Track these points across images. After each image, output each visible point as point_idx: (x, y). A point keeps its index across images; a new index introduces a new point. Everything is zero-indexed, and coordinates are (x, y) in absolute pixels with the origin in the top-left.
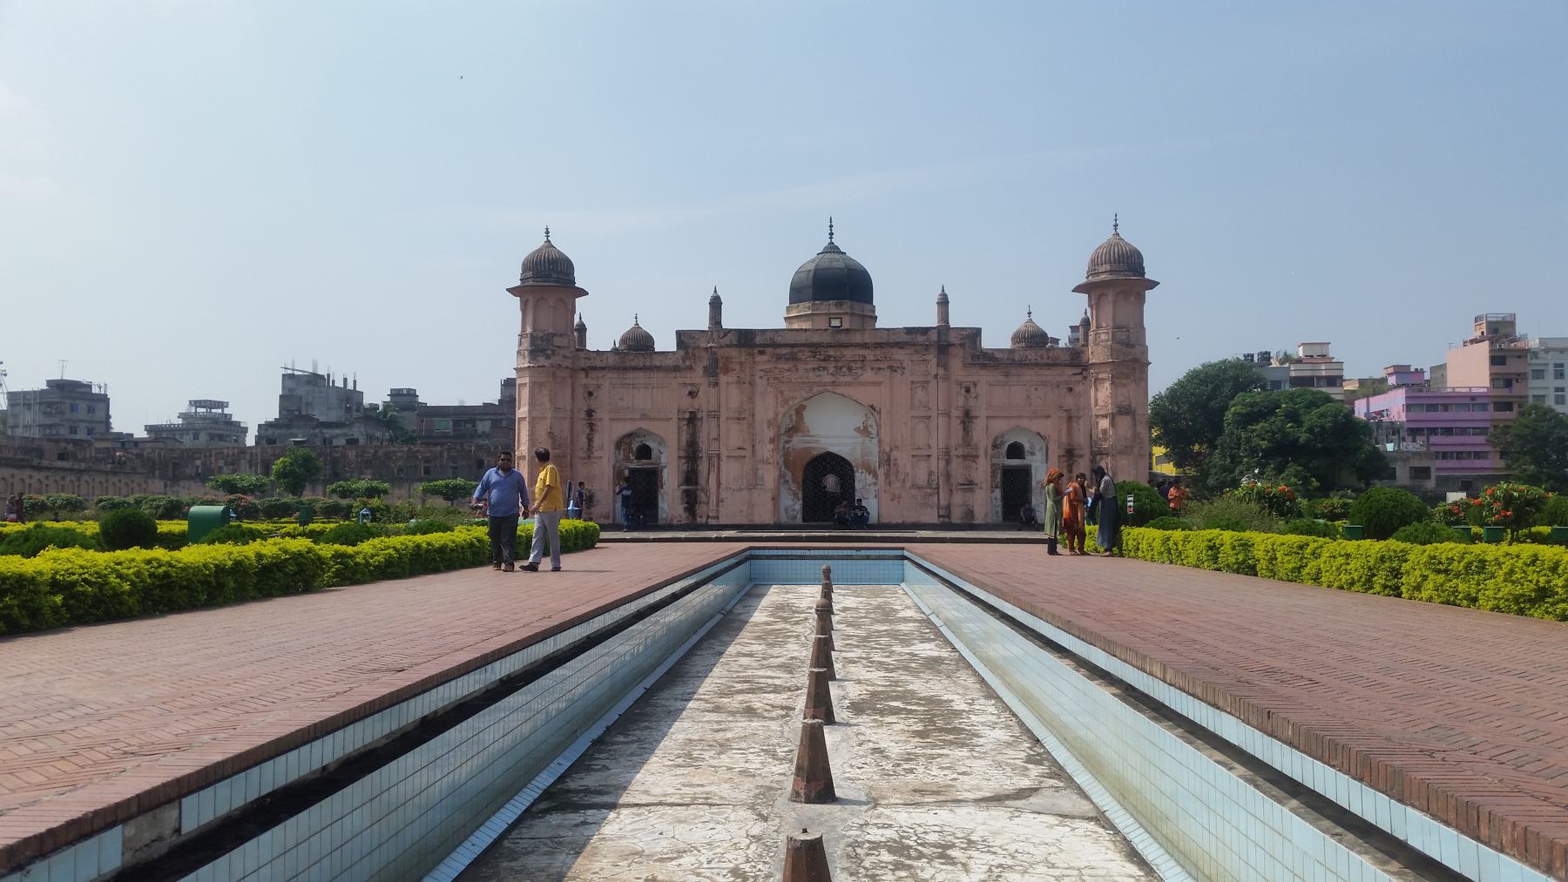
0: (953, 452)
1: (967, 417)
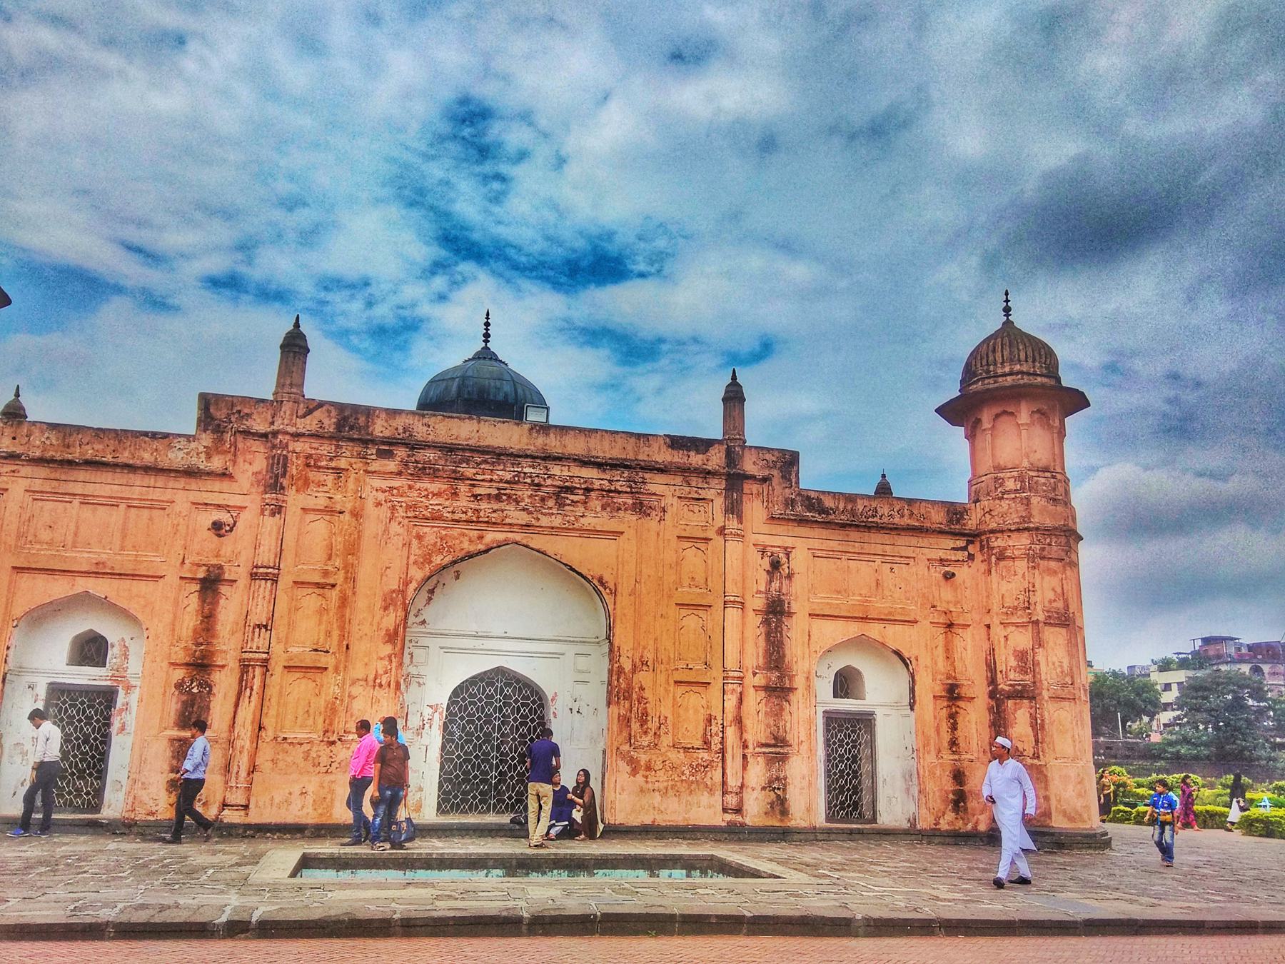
0: (751, 681)
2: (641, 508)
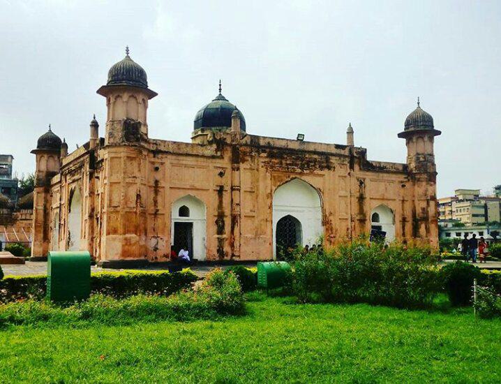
1: (361, 198)
2: (329, 168)
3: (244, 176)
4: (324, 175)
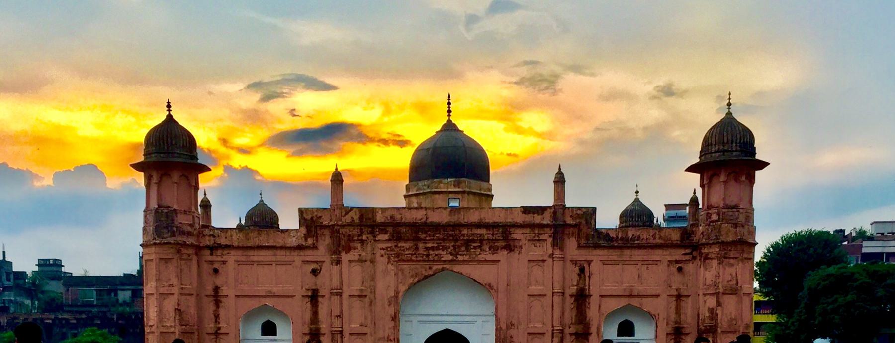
2: (509, 248)
3: (350, 274)
4: (499, 261)
